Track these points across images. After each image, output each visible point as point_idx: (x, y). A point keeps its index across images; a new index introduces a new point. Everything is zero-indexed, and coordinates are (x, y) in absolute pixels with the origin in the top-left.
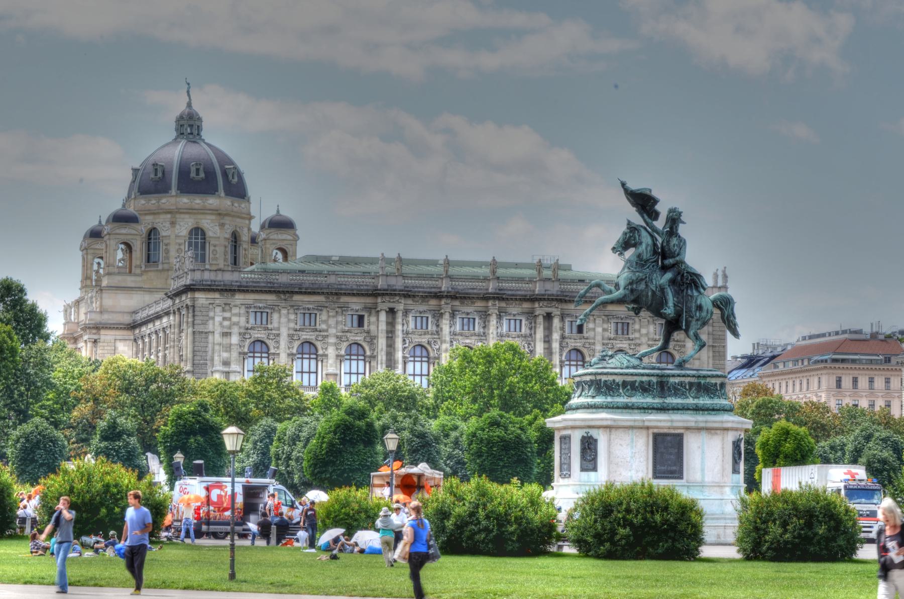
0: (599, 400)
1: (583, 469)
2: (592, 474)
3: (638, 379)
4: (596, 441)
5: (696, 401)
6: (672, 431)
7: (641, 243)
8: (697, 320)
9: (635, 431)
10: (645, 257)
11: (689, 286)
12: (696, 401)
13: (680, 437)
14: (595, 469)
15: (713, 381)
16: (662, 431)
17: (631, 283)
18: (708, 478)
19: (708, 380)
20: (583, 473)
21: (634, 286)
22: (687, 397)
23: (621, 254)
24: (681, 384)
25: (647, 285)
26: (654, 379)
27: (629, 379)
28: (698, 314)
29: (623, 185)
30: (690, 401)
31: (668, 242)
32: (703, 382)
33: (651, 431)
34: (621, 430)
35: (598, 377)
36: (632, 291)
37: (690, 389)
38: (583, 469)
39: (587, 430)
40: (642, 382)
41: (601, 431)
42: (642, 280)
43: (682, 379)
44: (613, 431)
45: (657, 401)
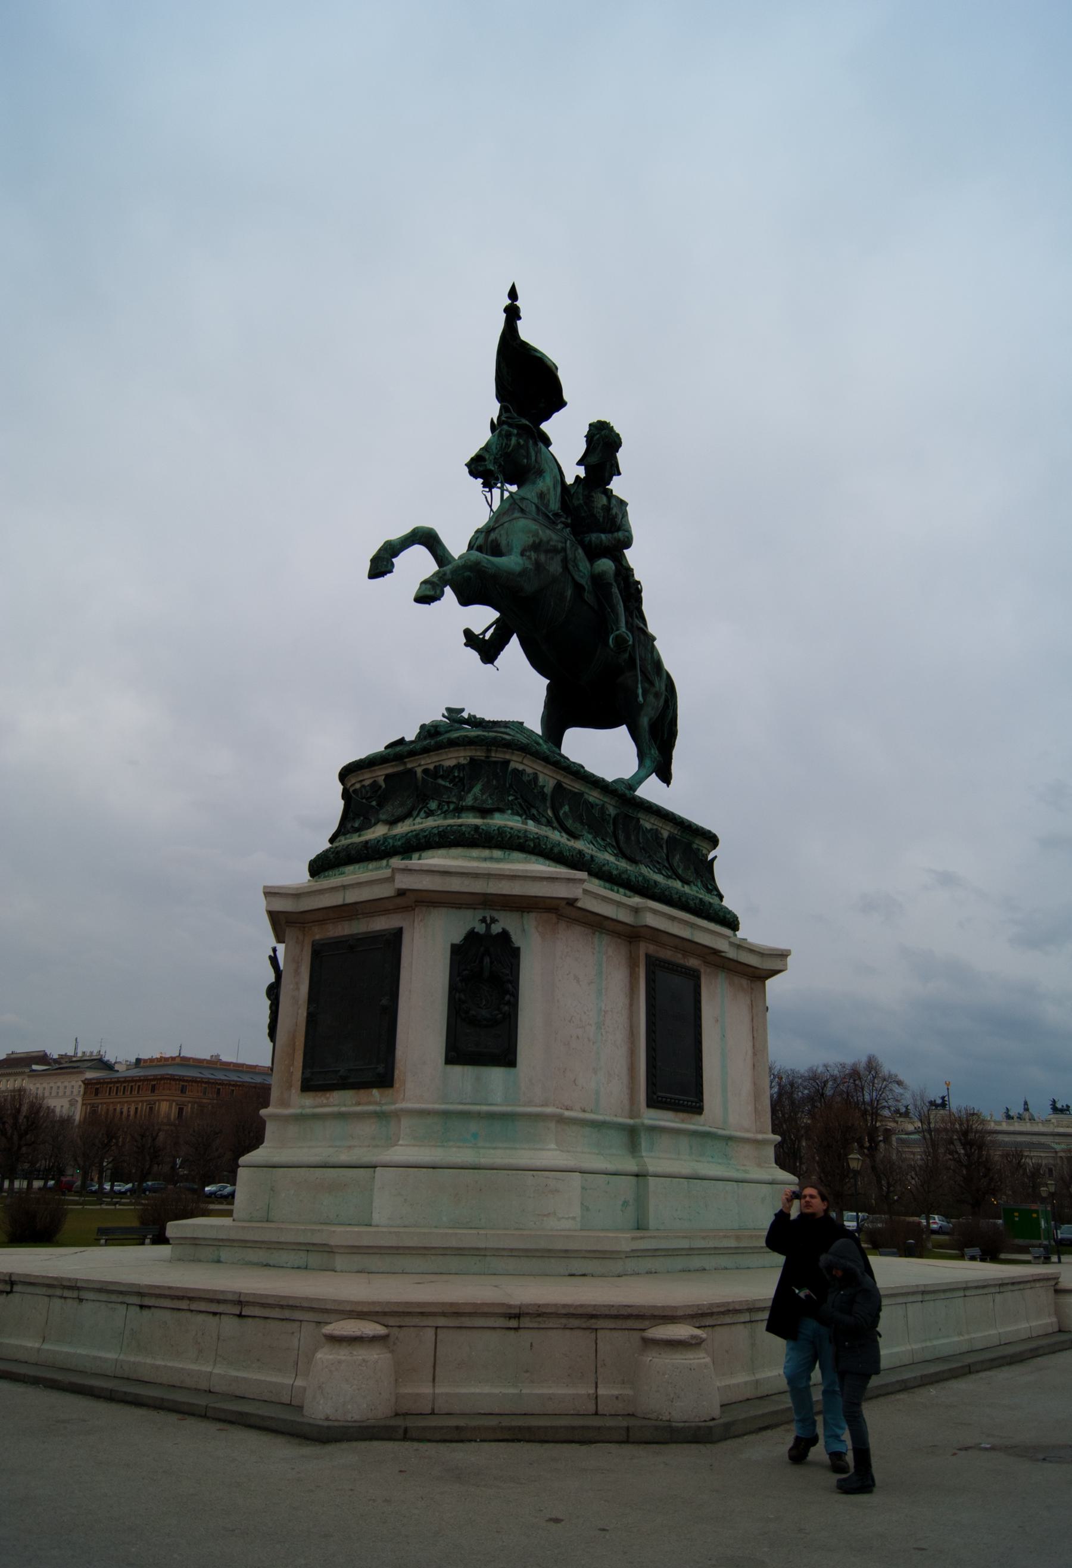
0: (508, 821)
1: (458, 1053)
2: (496, 1075)
4: (516, 953)
7: (540, 473)
14: (507, 1058)
17: (536, 547)
20: (457, 1069)
21: (542, 558)
23: (488, 485)
25: (566, 568)
29: (512, 313)
31: (589, 500)
33: (644, 949)
35: (498, 756)
36: (538, 566)
38: (458, 1053)
39: (488, 914)
41: (531, 921)
42: (555, 551)
45: (623, 864)
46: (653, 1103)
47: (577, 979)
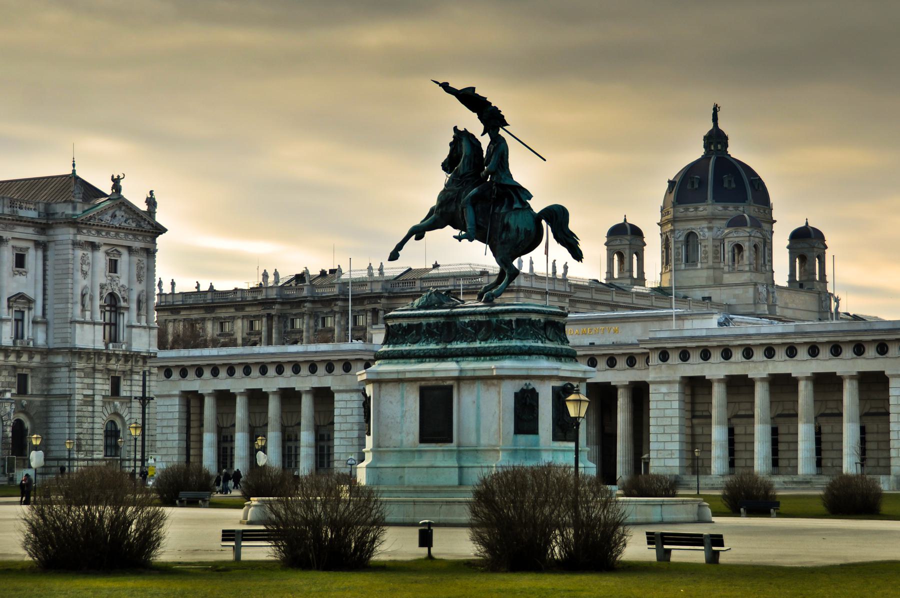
3: (424, 321)
5: (484, 344)
6: (441, 383)
8: (502, 243)
9: (406, 384)
10: (461, 172)
11: (499, 201)
12: (484, 344)
13: (450, 388)
15: (507, 318)
16: (430, 384)
18: (485, 441)
19: (501, 317)
22: (475, 341)
24: (471, 323)
26: (442, 320)
27: (415, 322)
28: (504, 236)
30: (477, 344)
32: (494, 320)
34: (391, 385)
37: (480, 329)
40: (428, 325)
42: (452, 200)
43: (473, 318)
44: (383, 385)
46: (423, 440)
47: (391, 402)
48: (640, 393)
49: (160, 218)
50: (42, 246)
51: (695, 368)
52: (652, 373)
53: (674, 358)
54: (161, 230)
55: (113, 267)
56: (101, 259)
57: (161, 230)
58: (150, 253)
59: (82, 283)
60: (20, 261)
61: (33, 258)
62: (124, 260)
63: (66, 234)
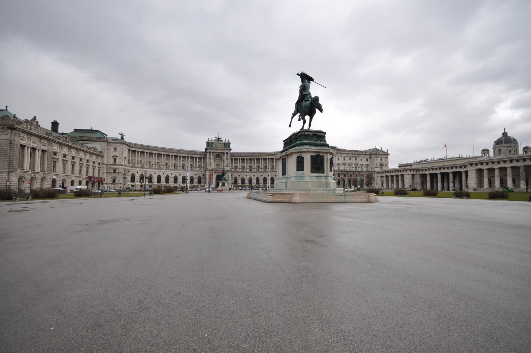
48: (466, 173)
49: (389, 153)
50: (371, 158)
51: (479, 167)
52: (469, 168)
53: (474, 165)
54: (389, 154)
55: (381, 160)
56: (379, 159)
57: (389, 154)
58: (387, 158)
59: (376, 162)
60: (367, 160)
61: (369, 159)
62: (383, 159)
63: (373, 156)
